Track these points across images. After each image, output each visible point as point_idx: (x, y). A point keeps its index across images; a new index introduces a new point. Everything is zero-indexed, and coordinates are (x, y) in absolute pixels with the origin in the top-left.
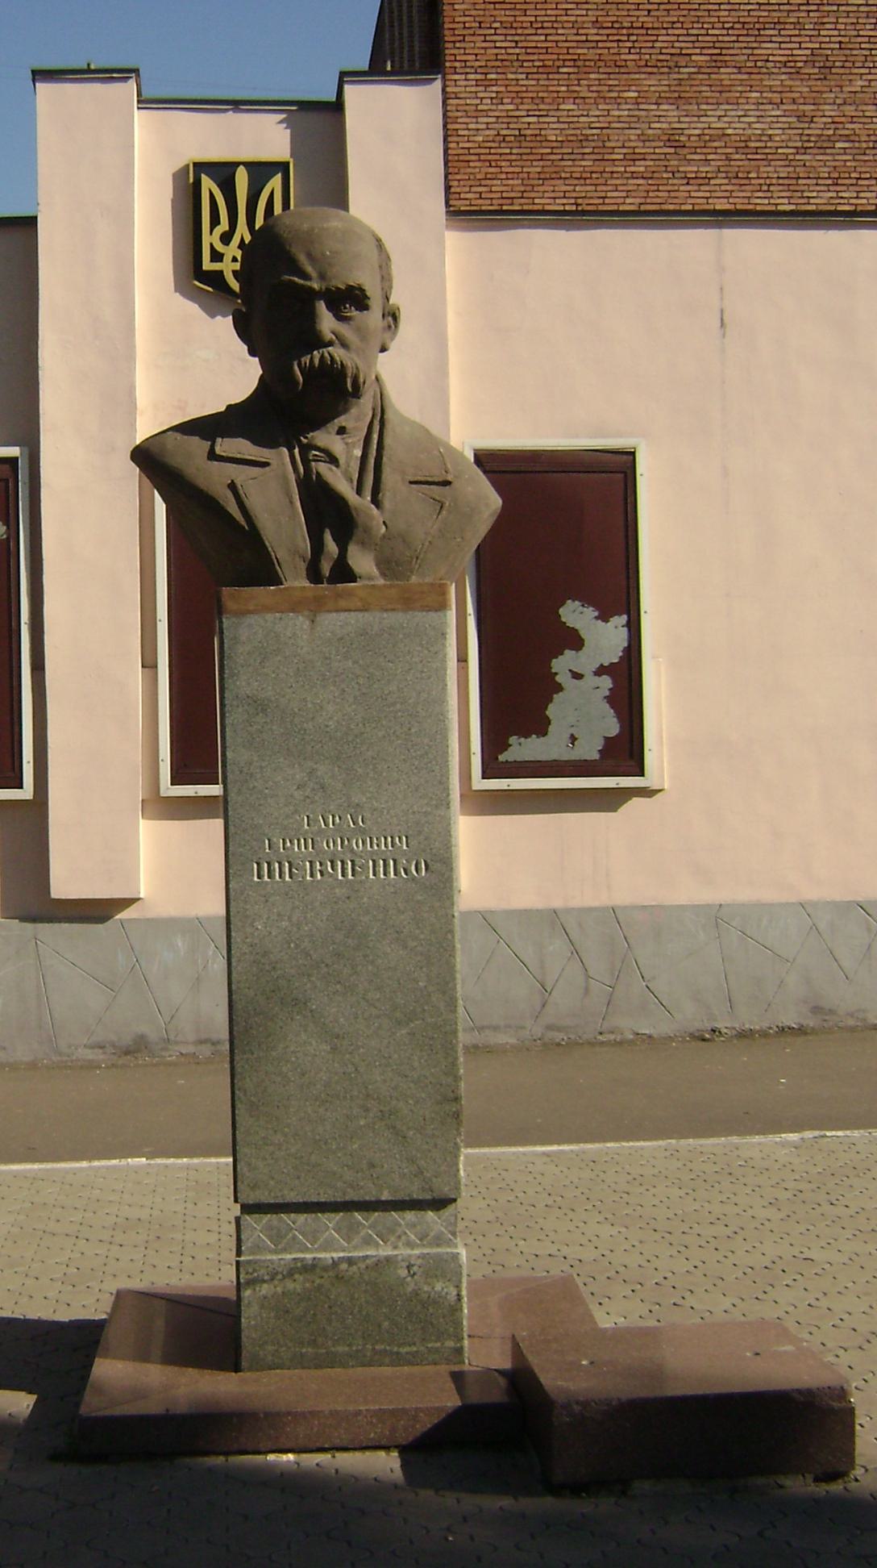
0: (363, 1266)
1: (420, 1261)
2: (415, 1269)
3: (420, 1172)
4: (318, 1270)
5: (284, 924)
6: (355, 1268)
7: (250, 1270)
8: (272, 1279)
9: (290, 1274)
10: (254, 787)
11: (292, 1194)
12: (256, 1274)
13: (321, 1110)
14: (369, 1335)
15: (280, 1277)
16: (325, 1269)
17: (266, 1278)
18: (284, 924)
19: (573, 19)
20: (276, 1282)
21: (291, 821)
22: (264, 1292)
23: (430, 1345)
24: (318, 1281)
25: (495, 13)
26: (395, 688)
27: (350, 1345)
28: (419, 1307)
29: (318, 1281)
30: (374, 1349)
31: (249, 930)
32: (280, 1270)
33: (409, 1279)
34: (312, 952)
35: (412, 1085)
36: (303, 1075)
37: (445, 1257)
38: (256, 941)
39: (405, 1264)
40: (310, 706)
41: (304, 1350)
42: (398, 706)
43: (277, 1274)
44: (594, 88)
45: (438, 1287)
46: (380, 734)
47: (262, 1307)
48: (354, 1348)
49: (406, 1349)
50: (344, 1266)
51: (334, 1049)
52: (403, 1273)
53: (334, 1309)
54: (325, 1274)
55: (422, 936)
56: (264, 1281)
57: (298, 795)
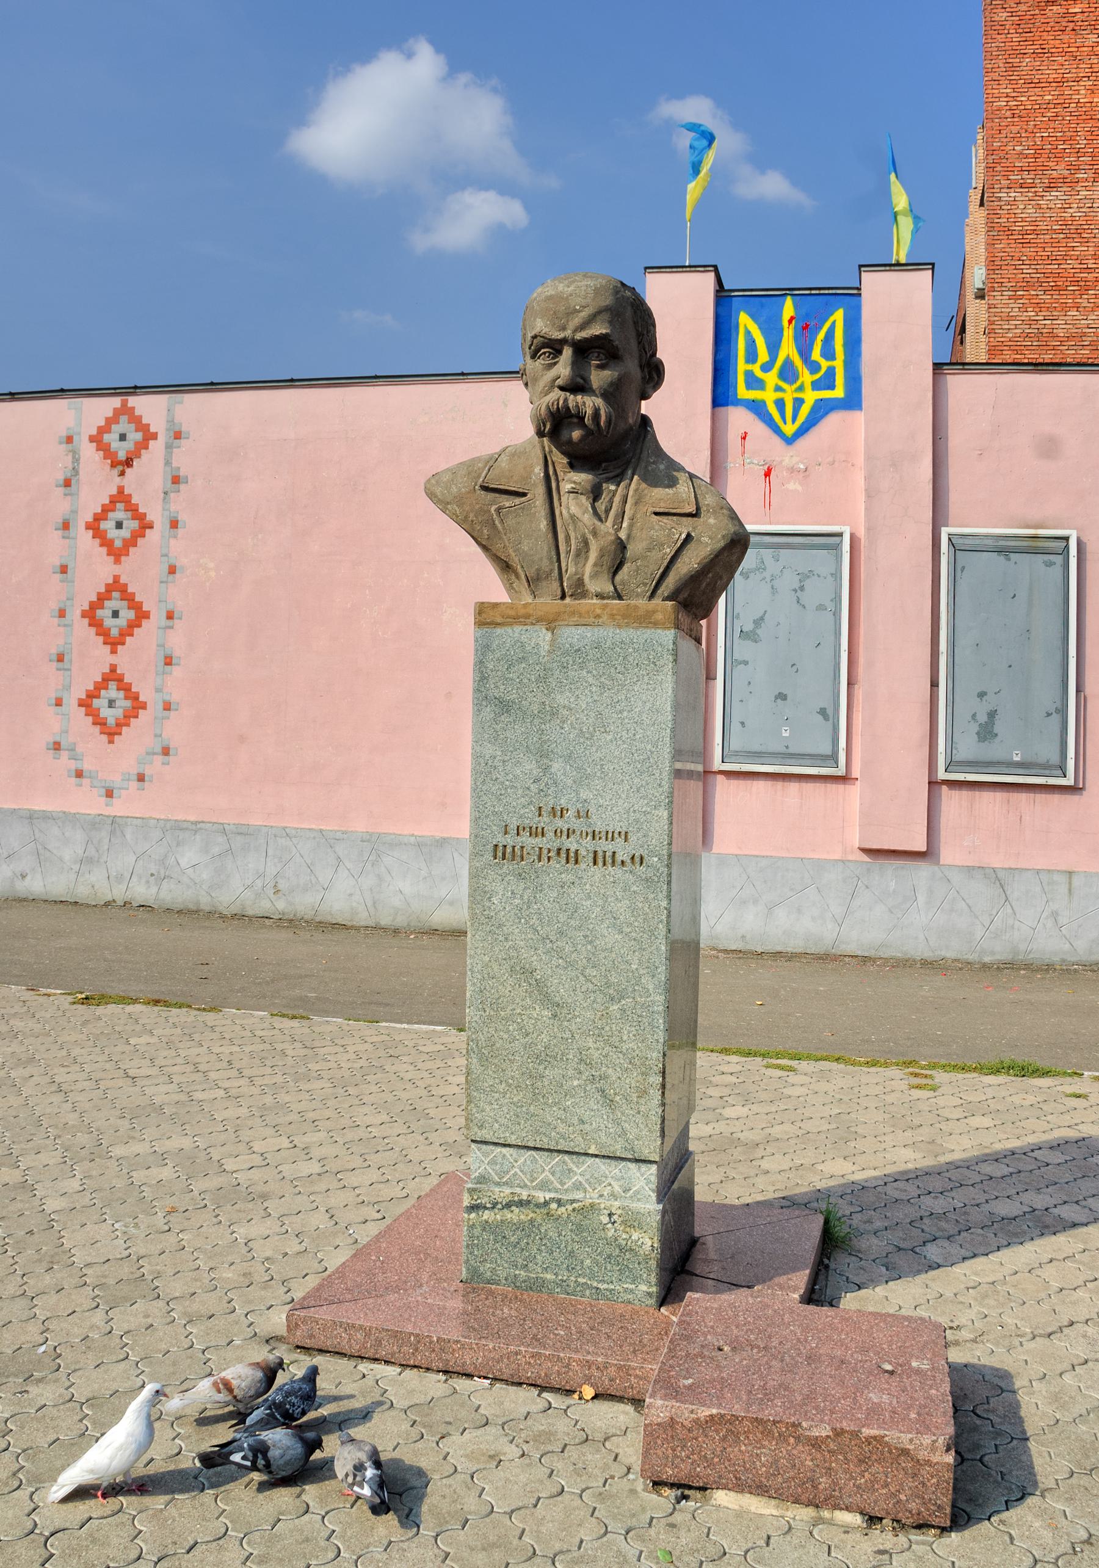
0: (570, 1208)
1: (619, 1212)
2: (615, 1217)
3: (624, 1132)
4: (532, 1206)
5: (517, 901)
6: (563, 1209)
7: (475, 1197)
8: (493, 1208)
9: (508, 1206)
10: (497, 779)
11: (514, 1137)
12: (479, 1201)
13: (541, 1067)
14: (573, 1269)
15: (500, 1206)
16: (538, 1206)
17: (488, 1205)
18: (517, 901)
19: (1078, 253)
20: (496, 1211)
21: (527, 810)
22: (485, 1217)
23: (625, 1286)
24: (532, 1215)
25: (1024, 250)
26: (623, 697)
27: (556, 1274)
28: (617, 1251)
29: (532, 1215)
30: (576, 1281)
31: (487, 904)
32: (500, 1200)
33: (610, 1225)
34: (539, 928)
35: (621, 1055)
36: (527, 1035)
37: (642, 1211)
38: (492, 914)
39: (606, 1212)
40: (548, 708)
41: (517, 1272)
42: (625, 714)
43: (497, 1203)
44: (1092, 301)
45: (635, 1236)
46: (609, 738)
47: (484, 1229)
48: (560, 1278)
49: (605, 1286)
50: (554, 1206)
51: (555, 1016)
52: (605, 1219)
53: (544, 1242)
54: (538, 1210)
55: (636, 924)
56: (485, 1208)
57: (534, 788)
